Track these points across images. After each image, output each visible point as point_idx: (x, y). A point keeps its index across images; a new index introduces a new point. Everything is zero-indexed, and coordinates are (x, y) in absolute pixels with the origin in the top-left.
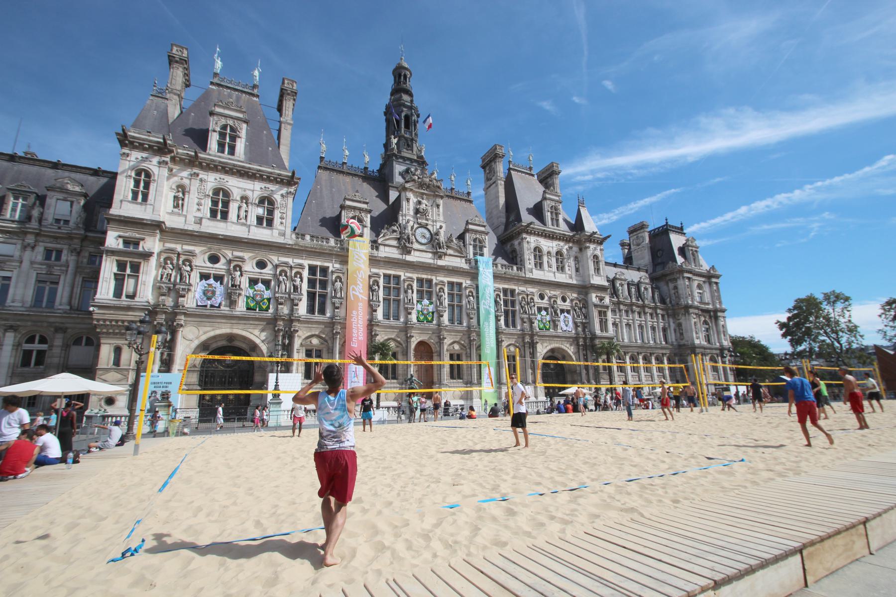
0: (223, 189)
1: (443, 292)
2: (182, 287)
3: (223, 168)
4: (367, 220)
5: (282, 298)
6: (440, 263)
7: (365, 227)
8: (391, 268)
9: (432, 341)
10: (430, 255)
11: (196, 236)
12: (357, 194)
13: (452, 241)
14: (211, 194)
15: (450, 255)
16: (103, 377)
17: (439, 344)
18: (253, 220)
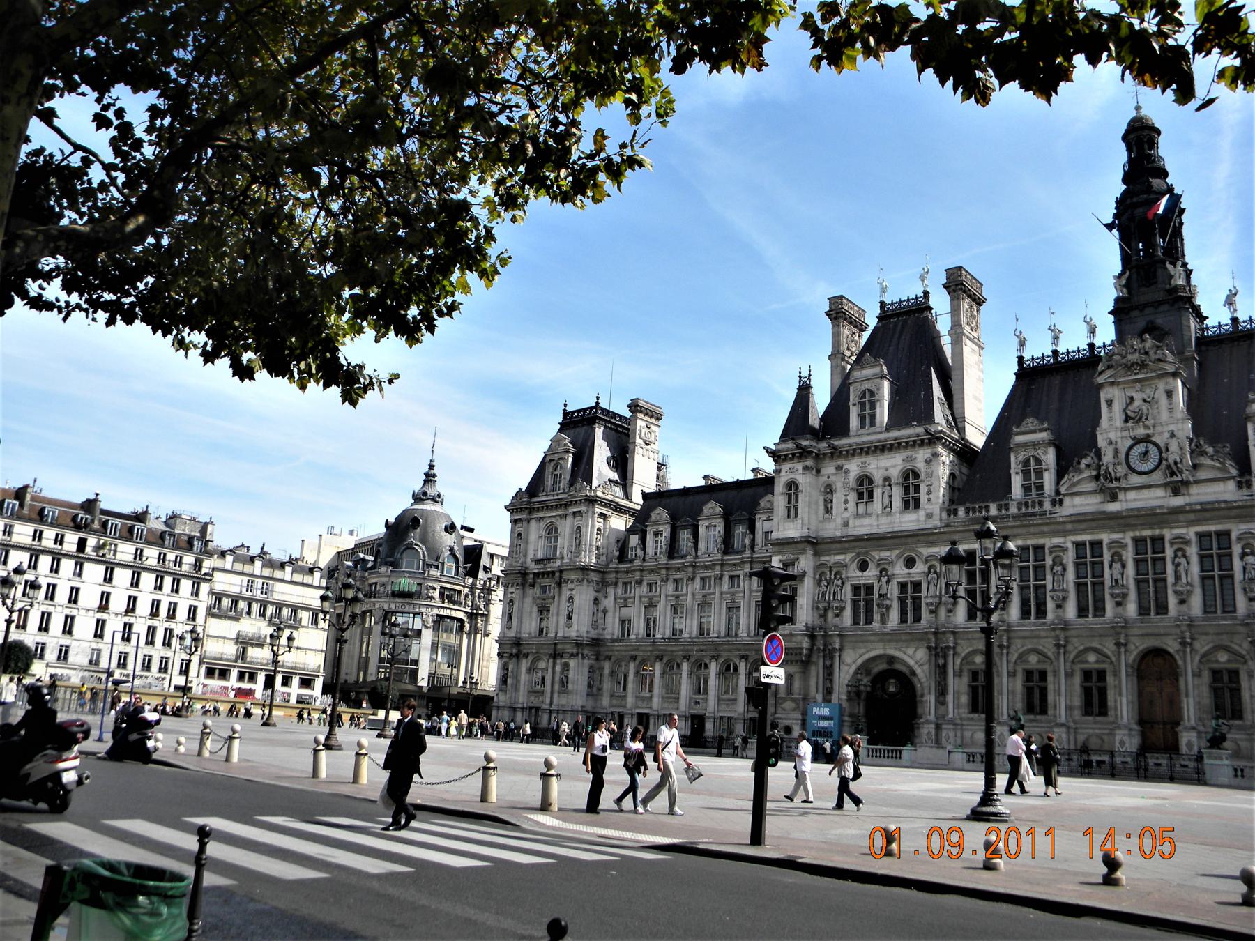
0: (867, 477)
1: (1184, 556)
2: (835, 605)
3: (861, 449)
4: (1049, 457)
5: (932, 604)
6: (1178, 501)
7: (1046, 470)
8: (1084, 531)
9: (1172, 646)
10: (1160, 492)
11: (846, 541)
12: (1030, 420)
13: (1206, 453)
14: (855, 486)
15: (1197, 482)
16: (783, 706)
17: (1181, 654)
18: (897, 503)
